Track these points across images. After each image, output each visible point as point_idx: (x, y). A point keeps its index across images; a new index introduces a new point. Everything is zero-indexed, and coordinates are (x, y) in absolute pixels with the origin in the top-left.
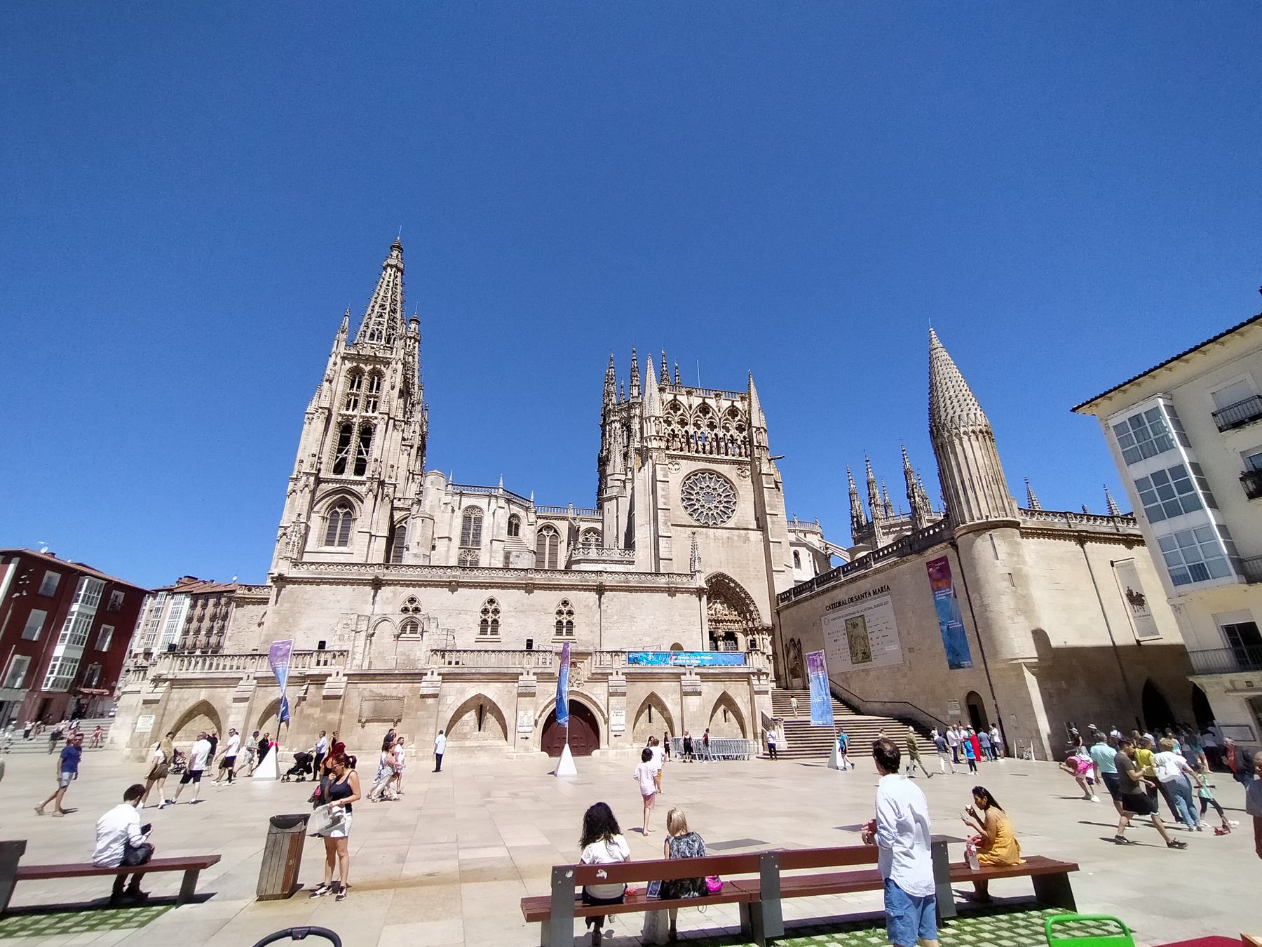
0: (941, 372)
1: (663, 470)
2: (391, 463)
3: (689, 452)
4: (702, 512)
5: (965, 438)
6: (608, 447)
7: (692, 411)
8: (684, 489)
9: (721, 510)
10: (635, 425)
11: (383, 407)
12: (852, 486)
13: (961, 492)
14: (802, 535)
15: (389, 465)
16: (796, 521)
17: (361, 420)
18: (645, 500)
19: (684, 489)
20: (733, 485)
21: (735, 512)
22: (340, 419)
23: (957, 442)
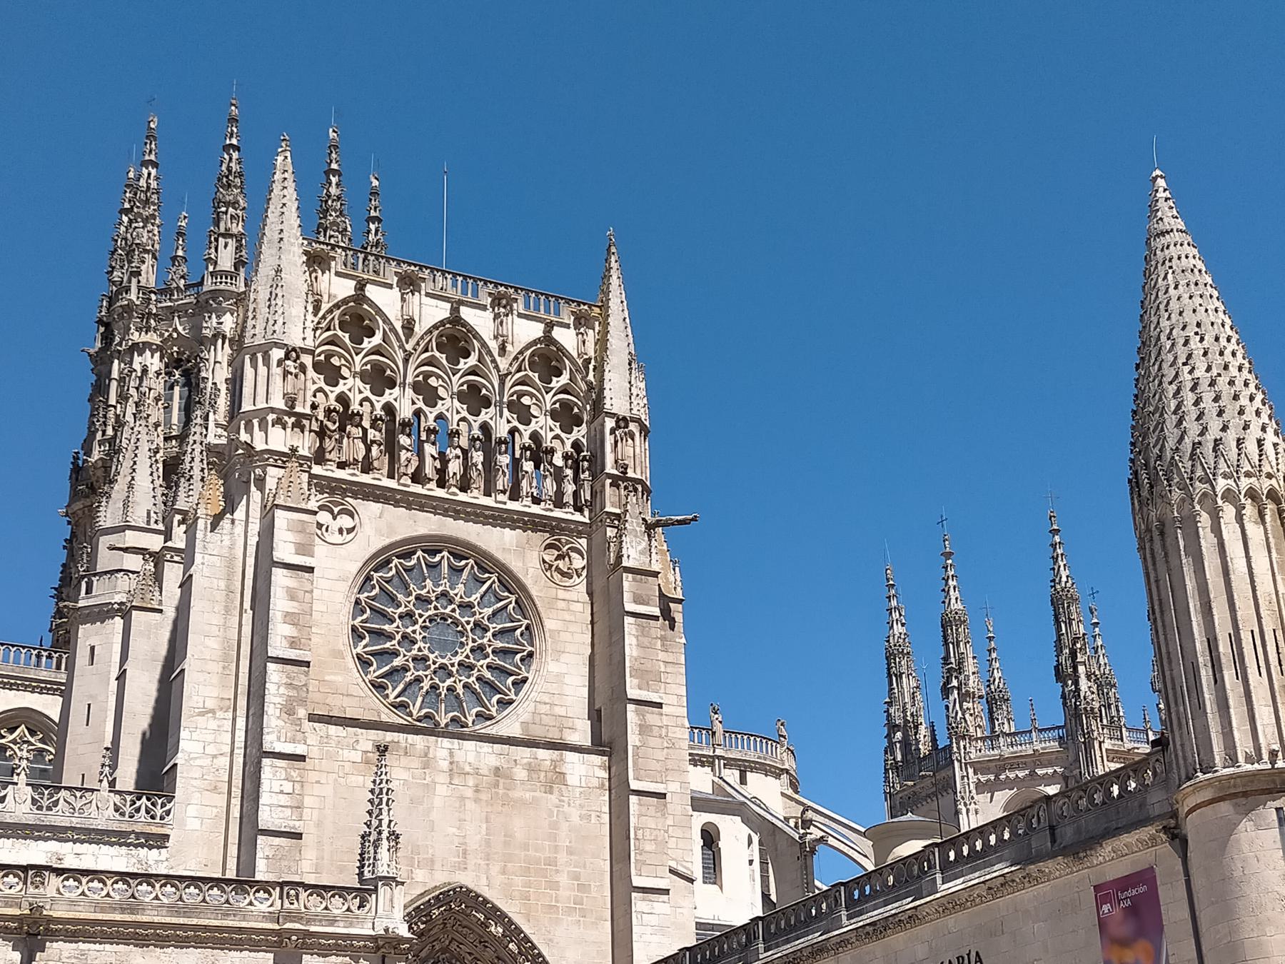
1: (301, 529)
3: (391, 476)
4: (418, 680)
6: (110, 432)
7: (412, 342)
8: (362, 597)
10: (217, 370)
12: (898, 629)
18: (226, 627)
19: (362, 597)
21: (527, 686)
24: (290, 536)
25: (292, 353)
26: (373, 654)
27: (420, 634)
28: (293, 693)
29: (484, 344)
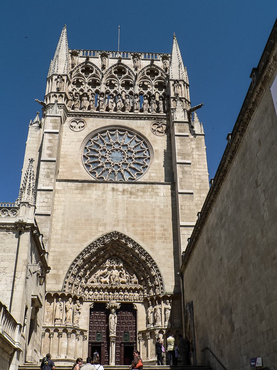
9: (130, 168)
19: (87, 147)
20: (147, 140)
24: (51, 124)
25: (60, 76)
26: (91, 163)
27: (108, 156)
28: (49, 171)
29: (130, 69)
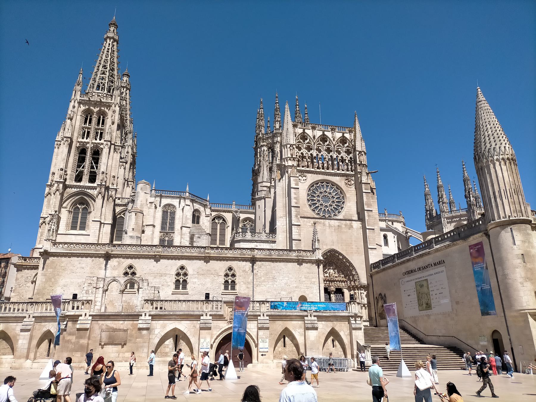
0: (483, 118)
1: (295, 180)
2: (113, 174)
3: (313, 168)
4: (321, 209)
5: (497, 163)
7: (315, 140)
8: (309, 193)
10: (277, 149)
11: (107, 137)
13: (493, 200)
14: (390, 223)
15: (112, 176)
16: (386, 213)
17: (92, 145)
18: (283, 201)
19: (309, 193)
22: (78, 145)
23: (492, 166)
25: (291, 145)
